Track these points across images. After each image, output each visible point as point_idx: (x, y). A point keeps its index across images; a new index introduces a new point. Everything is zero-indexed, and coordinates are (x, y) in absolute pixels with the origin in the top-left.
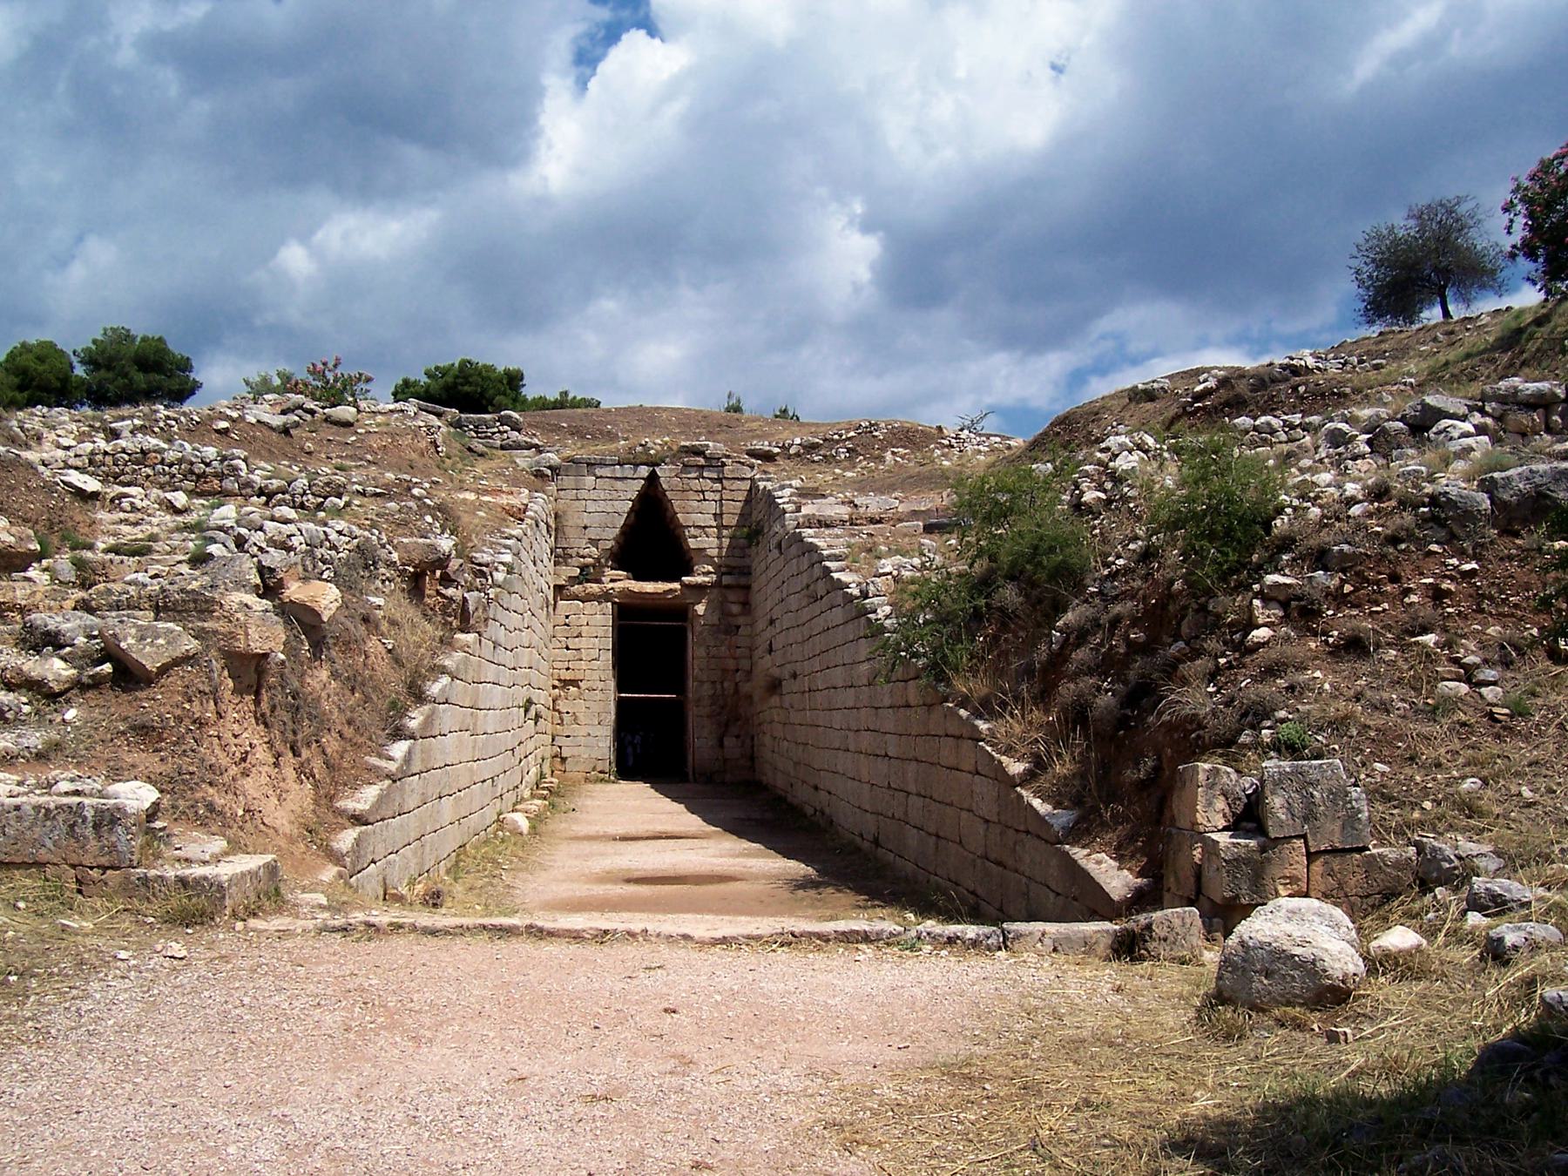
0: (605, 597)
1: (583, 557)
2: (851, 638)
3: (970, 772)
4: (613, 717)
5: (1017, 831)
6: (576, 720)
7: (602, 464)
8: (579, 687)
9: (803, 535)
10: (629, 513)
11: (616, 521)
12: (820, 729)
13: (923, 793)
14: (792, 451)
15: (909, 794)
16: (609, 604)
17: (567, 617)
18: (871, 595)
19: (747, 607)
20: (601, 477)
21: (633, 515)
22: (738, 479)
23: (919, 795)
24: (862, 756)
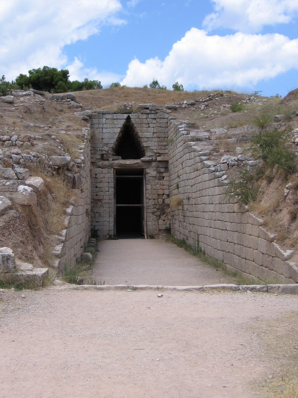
0: (111, 166)
2: (212, 186)
3: (257, 236)
5: (273, 257)
7: (108, 113)
8: (101, 202)
13: (240, 243)
14: (183, 106)
16: (112, 169)
17: (96, 175)
18: (219, 171)
19: (167, 169)
20: (108, 119)
21: (121, 133)
22: (162, 118)
23: (238, 244)
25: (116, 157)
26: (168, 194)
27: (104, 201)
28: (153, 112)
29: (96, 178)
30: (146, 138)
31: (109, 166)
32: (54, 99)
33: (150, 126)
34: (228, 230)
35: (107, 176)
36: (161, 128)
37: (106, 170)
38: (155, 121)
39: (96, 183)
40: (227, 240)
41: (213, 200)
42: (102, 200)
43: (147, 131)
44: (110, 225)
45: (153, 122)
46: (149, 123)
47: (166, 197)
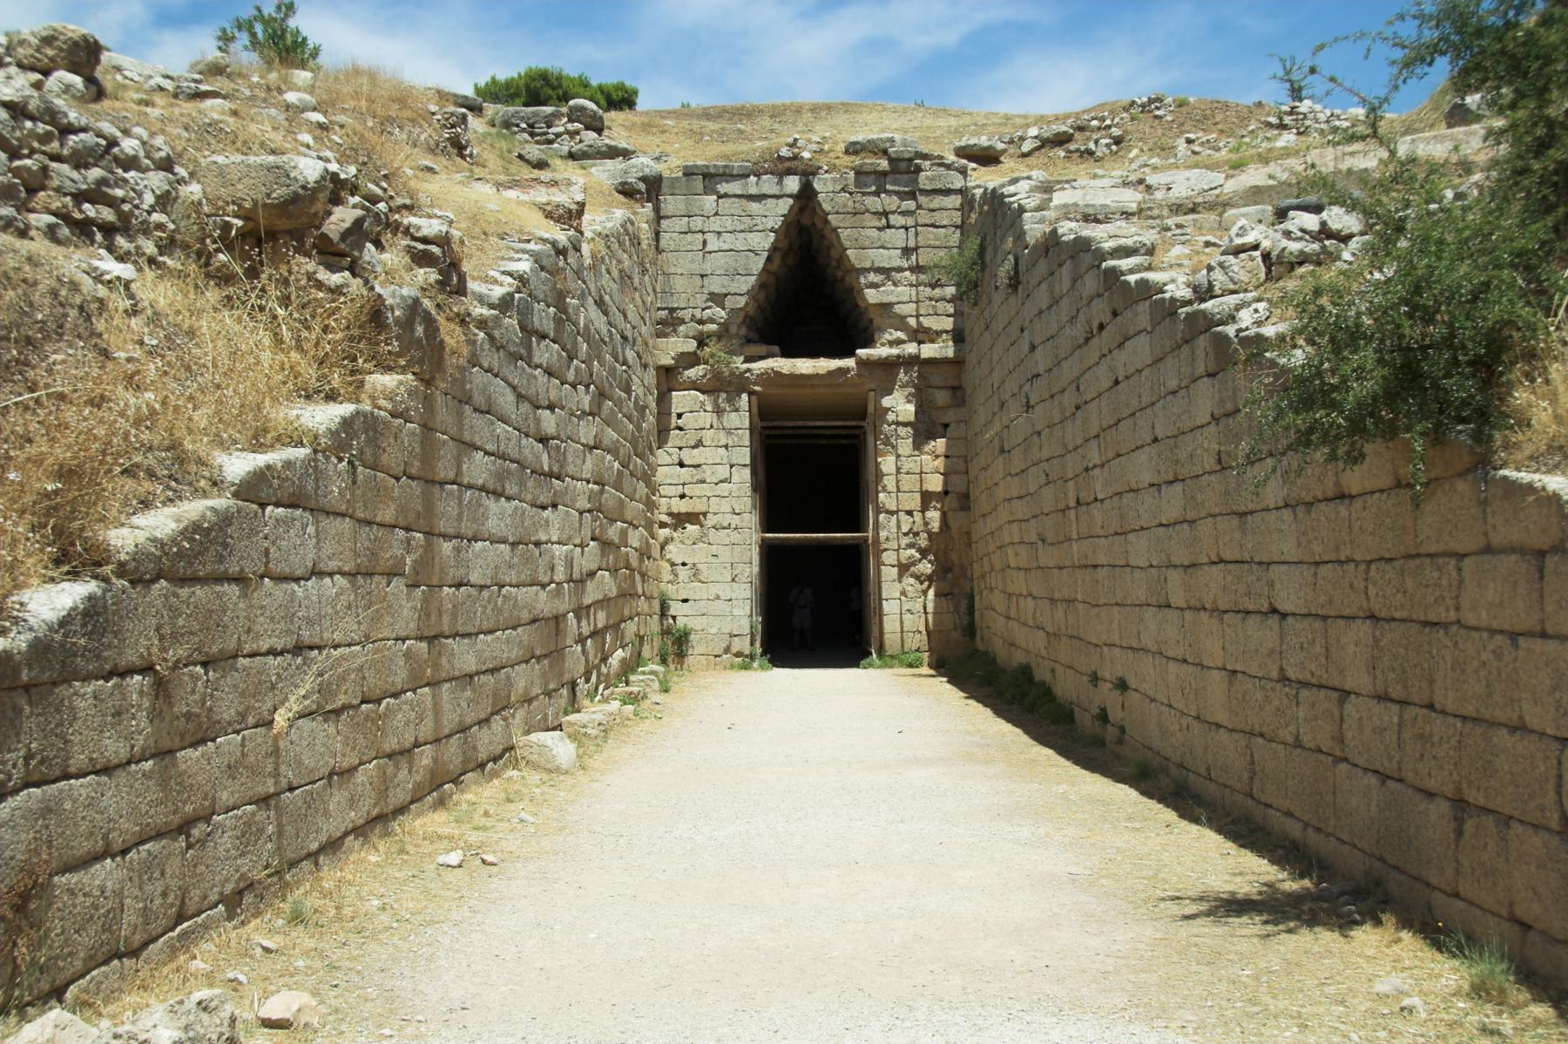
1: (701, 322)
4: (756, 569)
6: (696, 575)
7: (728, 175)
9: (1060, 231)
12: (1101, 572)
13: (1396, 691)
15: (1345, 694)
16: (745, 396)
18: (1217, 291)
19: (959, 394)
20: (726, 196)
23: (1383, 698)
24: (1204, 616)
25: (761, 349)
26: (963, 489)
27: (711, 520)
29: (681, 429)
32: (518, 126)
33: (892, 222)
34: (1285, 607)
36: (935, 230)
40: (1282, 669)
41: (1182, 455)
42: (705, 514)
43: (879, 244)
44: (736, 612)
46: (887, 209)
47: (956, 505)
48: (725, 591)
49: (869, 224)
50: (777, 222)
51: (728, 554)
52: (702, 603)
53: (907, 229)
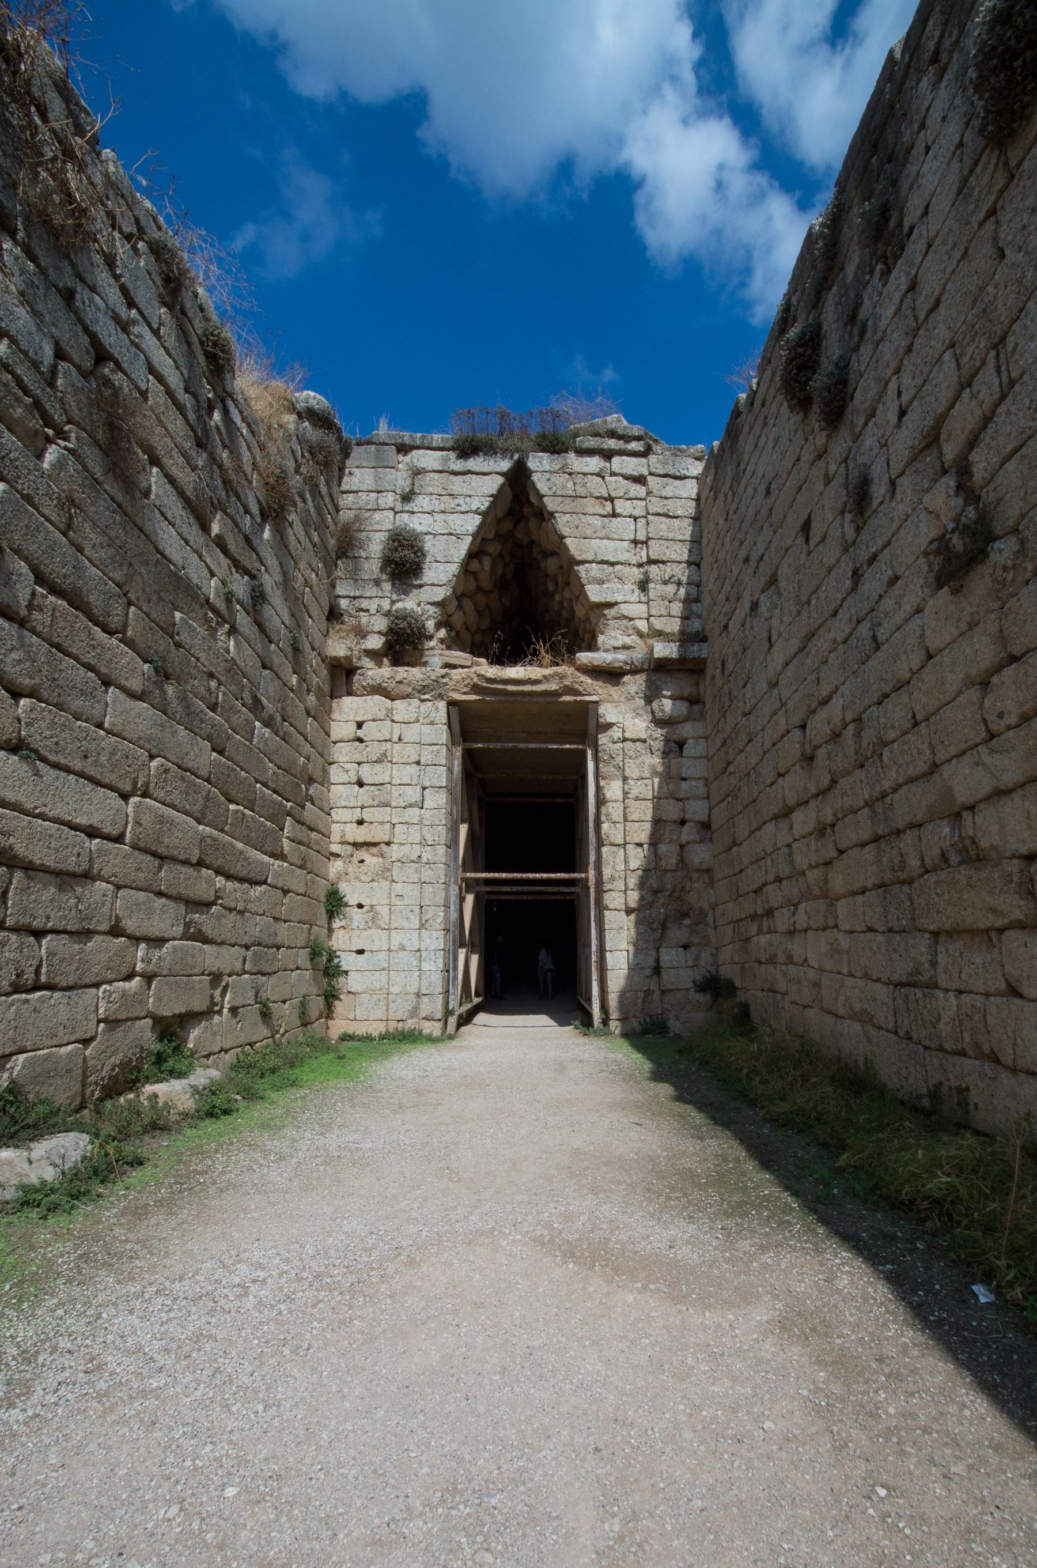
6: (373, 921)
10: (475, 536)
11: (453, 551)
16: (442, 705)
19: (696, 708)
25: (458, 656)
28: (634, 446)
29: (360, 740)
30: (603, 562)
31: (424, 689)
33: (618, 510)
35: (411, 733)
36: (668, 520)
37: (410, 708)
38: (640, 490)
39: (359, 764)
42: (388, 844)
43: (603, 534)
44: (425, 966)
45: (632, 495)
46: (613, 494)
47: (694, 836)
48: (410, 939)
49: (591, 511)
50: (484, 504)
51: (416, 893)
52: (383, 955)
53: (635, 520)
